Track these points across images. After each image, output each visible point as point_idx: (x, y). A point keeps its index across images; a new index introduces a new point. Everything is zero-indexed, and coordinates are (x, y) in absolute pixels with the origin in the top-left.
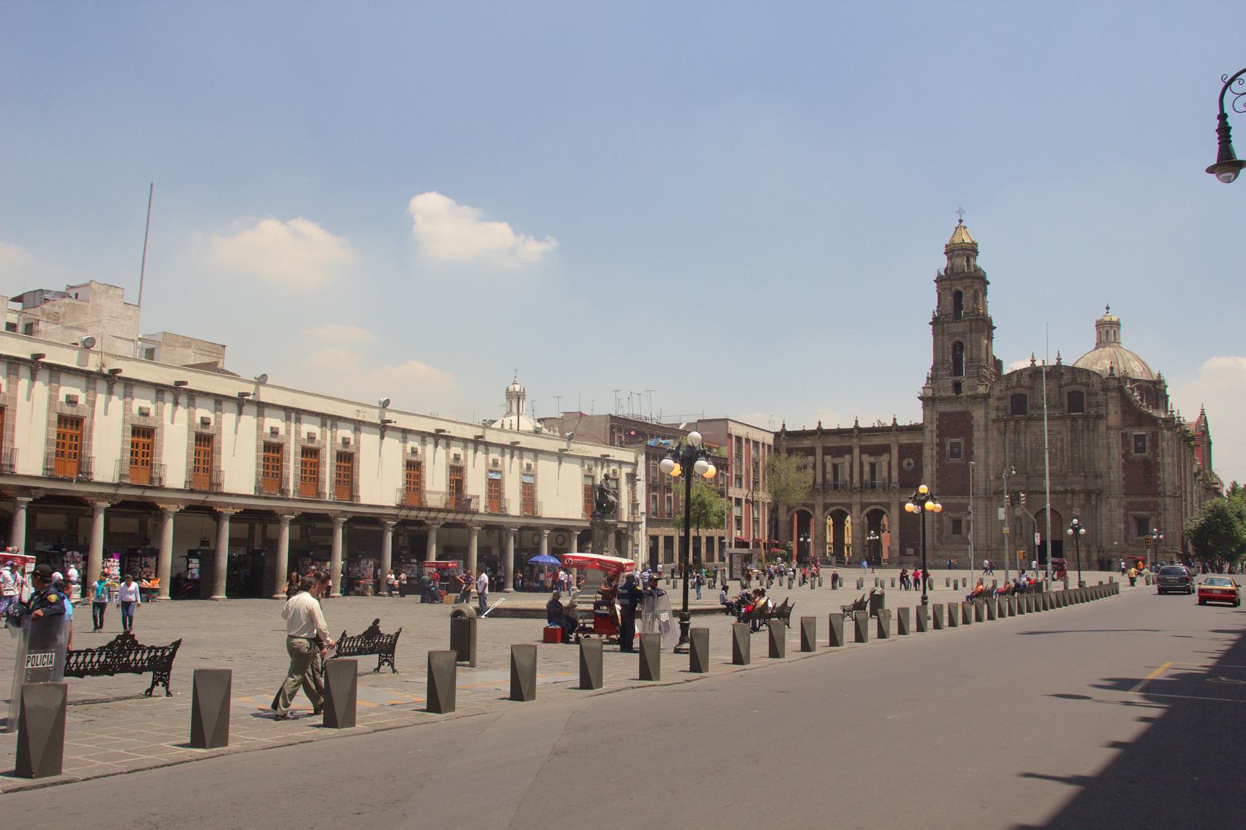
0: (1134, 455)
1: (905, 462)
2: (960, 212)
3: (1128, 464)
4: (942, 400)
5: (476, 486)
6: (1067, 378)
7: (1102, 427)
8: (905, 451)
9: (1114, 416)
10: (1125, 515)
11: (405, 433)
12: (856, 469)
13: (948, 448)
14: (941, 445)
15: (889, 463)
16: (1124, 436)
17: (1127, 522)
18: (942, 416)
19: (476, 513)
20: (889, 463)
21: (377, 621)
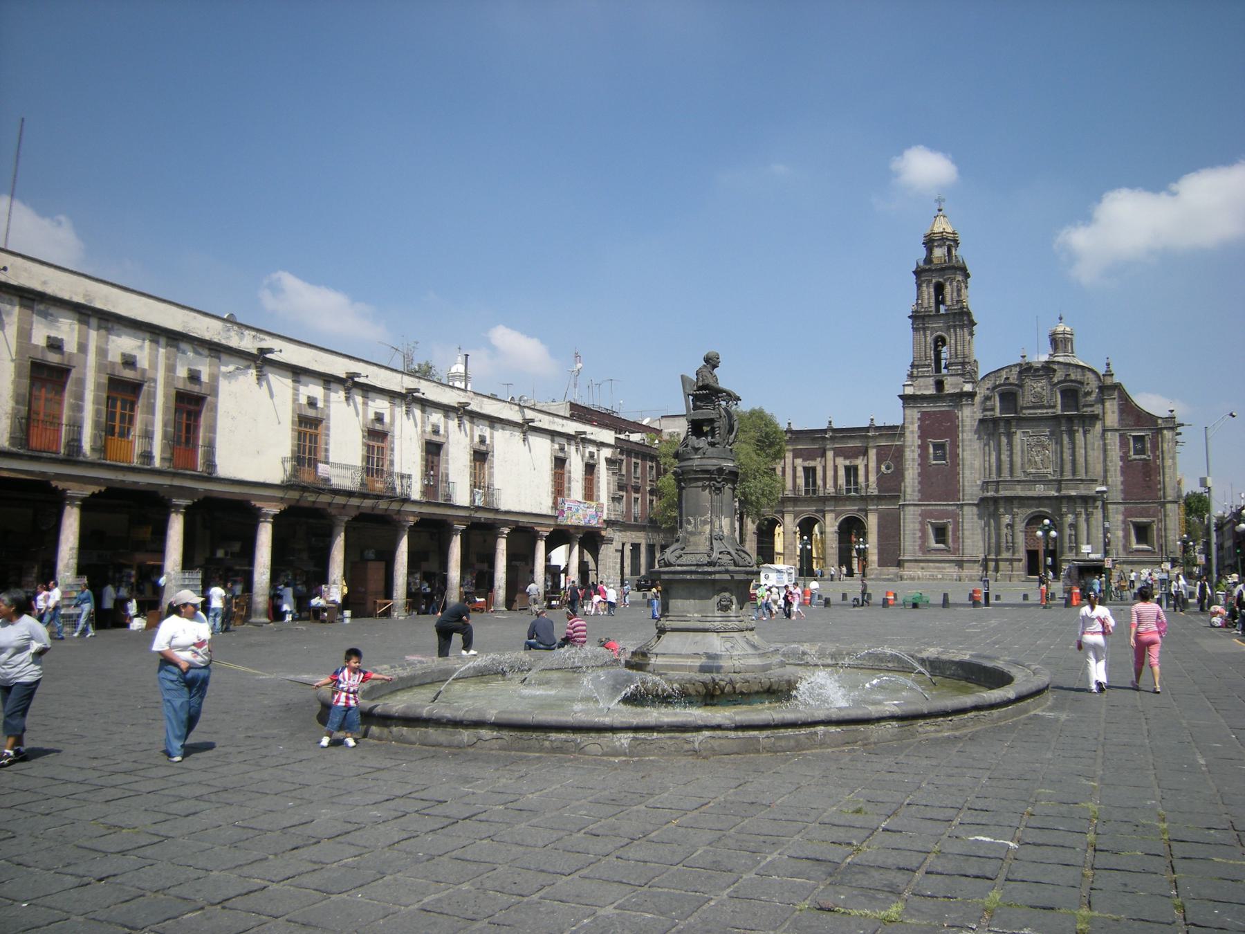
4: (924, 398)
5: (407, 458)
9: (1111, 413)
10: (1124, 522)
11: (298, 373)
12: (830, 473)
14: (923, 448)
15: (867, 466)
19: (406, 500)
20: (867, 466)
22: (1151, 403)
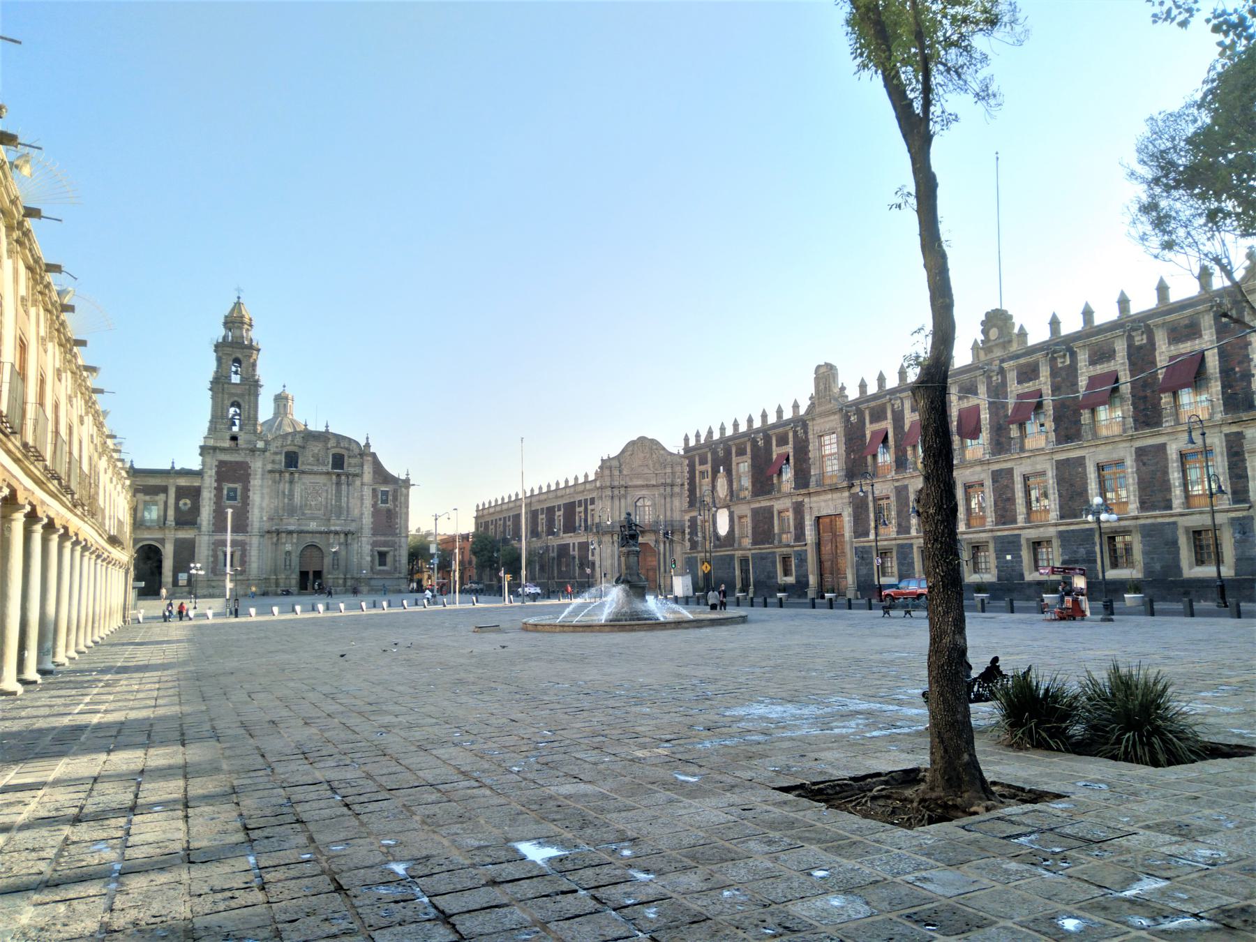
0: (380, 505)
1: (181, 503)
2: (239, 290)
3: (376, 512)
4: (223, 450)
6: (331, 443)
7: (358, 483)
8: (181, 492)
13: (225, 492)
14: (219, 489)
15: (166, 503)
16: (374, 490)
17: (372, 556)
18: (221, 464)
20: (166, 503)
21: (996, 660)
22: (393, 467)
